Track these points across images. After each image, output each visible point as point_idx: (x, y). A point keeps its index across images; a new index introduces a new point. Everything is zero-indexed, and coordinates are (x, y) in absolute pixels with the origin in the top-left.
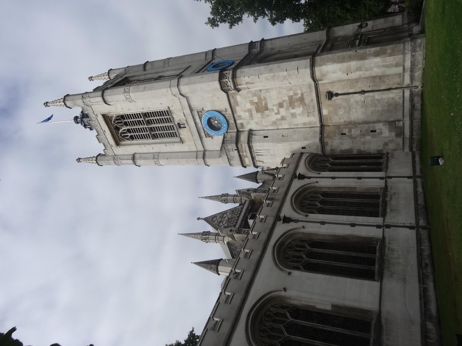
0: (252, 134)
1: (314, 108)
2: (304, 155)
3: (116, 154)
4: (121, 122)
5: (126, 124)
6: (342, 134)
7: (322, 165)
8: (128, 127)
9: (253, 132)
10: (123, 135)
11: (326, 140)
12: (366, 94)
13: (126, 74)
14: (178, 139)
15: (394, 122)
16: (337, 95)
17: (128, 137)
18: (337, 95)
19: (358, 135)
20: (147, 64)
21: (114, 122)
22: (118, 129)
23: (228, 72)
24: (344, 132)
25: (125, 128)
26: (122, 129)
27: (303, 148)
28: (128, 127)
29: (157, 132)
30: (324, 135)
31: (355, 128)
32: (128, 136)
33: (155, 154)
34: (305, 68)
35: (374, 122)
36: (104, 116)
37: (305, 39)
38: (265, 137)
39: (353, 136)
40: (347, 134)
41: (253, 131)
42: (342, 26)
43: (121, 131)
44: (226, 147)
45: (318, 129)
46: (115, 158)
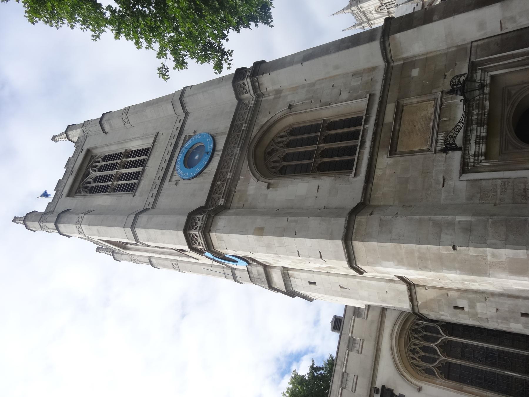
0: (289, 276)
2: (388, 313)
6: (455, 307)
7: (425, 344)
9: (289, 272)
13: (87, 137)
19: (492, 317)
20: (106, 115)
24: (460, 304)
30: (418, 302)
31: (482, 302)
33: (174, 263)
34: (337, 258)
37: (336, 67)
38: (311, 283)
39: (479, 316)
40: (466, 309)
41: (288, 269)
42: (415, 29)
46: (132, 259)
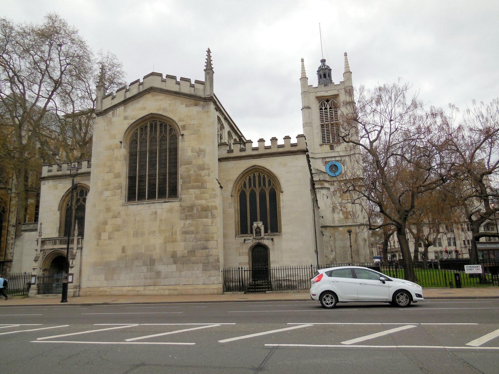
1: (342, 224)
4: (331, 105)
5: (330, 108)
8: (328, 109)
11: (328, 229)
12: (350, 248)
15: (336, 260)
16: (350, 235)
18: (350, 235)
22: (328, 101)
25: (328, 107)
27: (322, 217)
28: (328, 109)
29: (325, 128)
35: (335, 251)
43: (326, 103)
44: (321, 174)
45: (332, 225)
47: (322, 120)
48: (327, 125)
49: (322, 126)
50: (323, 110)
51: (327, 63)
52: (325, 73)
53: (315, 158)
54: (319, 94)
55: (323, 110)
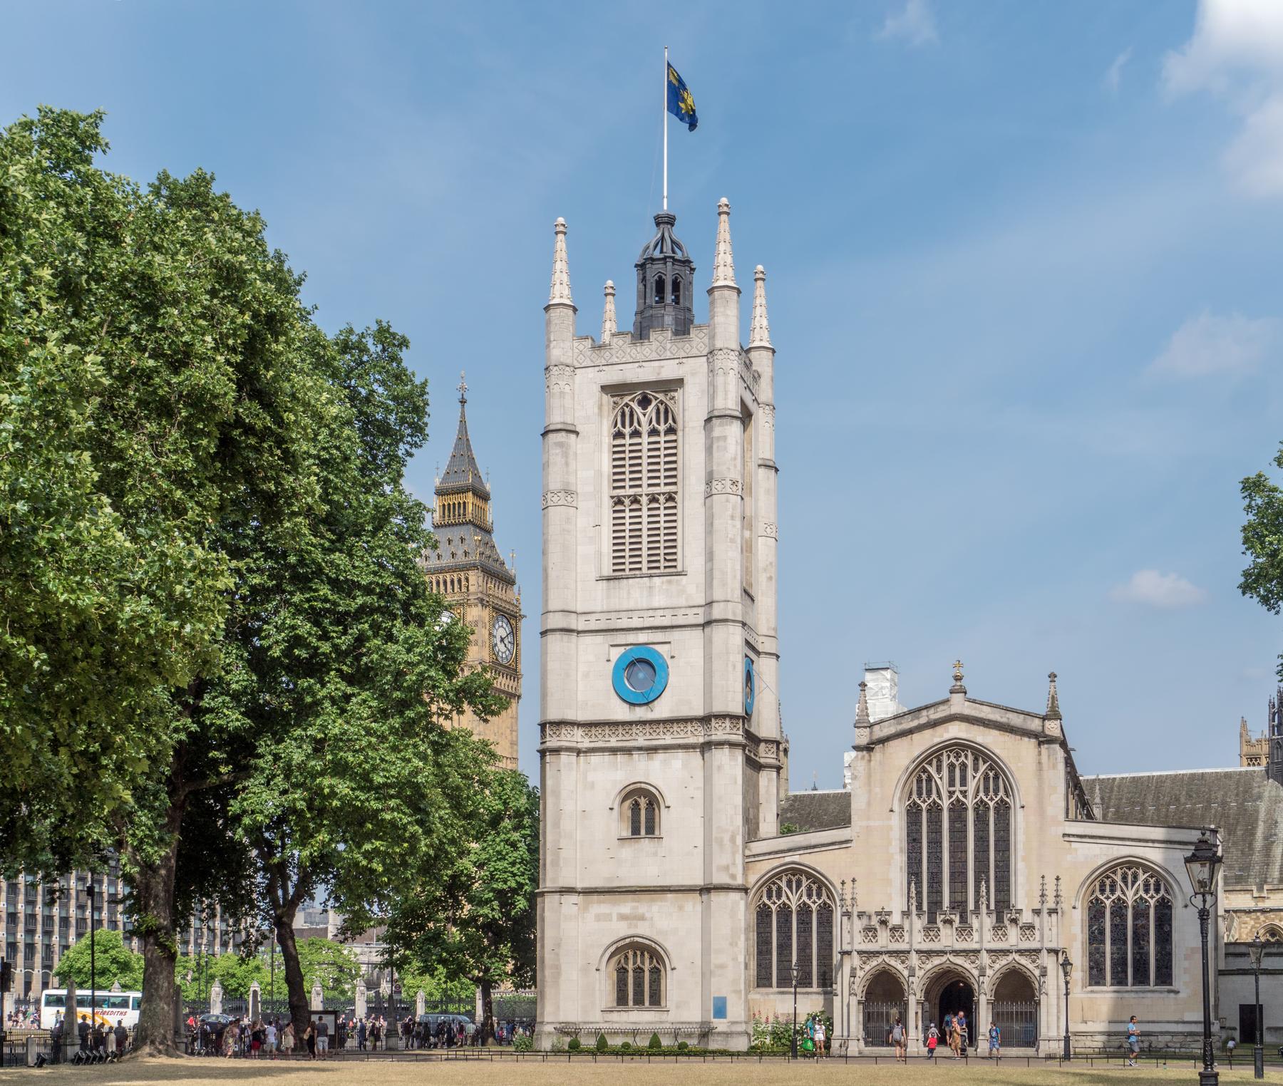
3: (577, 371)
5: (654, 432)
8: (645, 439)
10: (627, 410)
14: (607, 570)
17: (619, 425)
21: (662, 402)
22: (645, 402)
23: (741, 732)
25: (645, 429)
26: (641, 416)
28: (645, 439)
29: (627, 514)
32: (624, 426)
36: (679, 382)
43: (638, 410)
47: (617, 482)
48: (635, 500)
49: (619, 501)
50: (627, 437)
51: (677, 232)
52: (660, 277)
53: (579, 632)
54: (614, 376)
55: (627, 437)
